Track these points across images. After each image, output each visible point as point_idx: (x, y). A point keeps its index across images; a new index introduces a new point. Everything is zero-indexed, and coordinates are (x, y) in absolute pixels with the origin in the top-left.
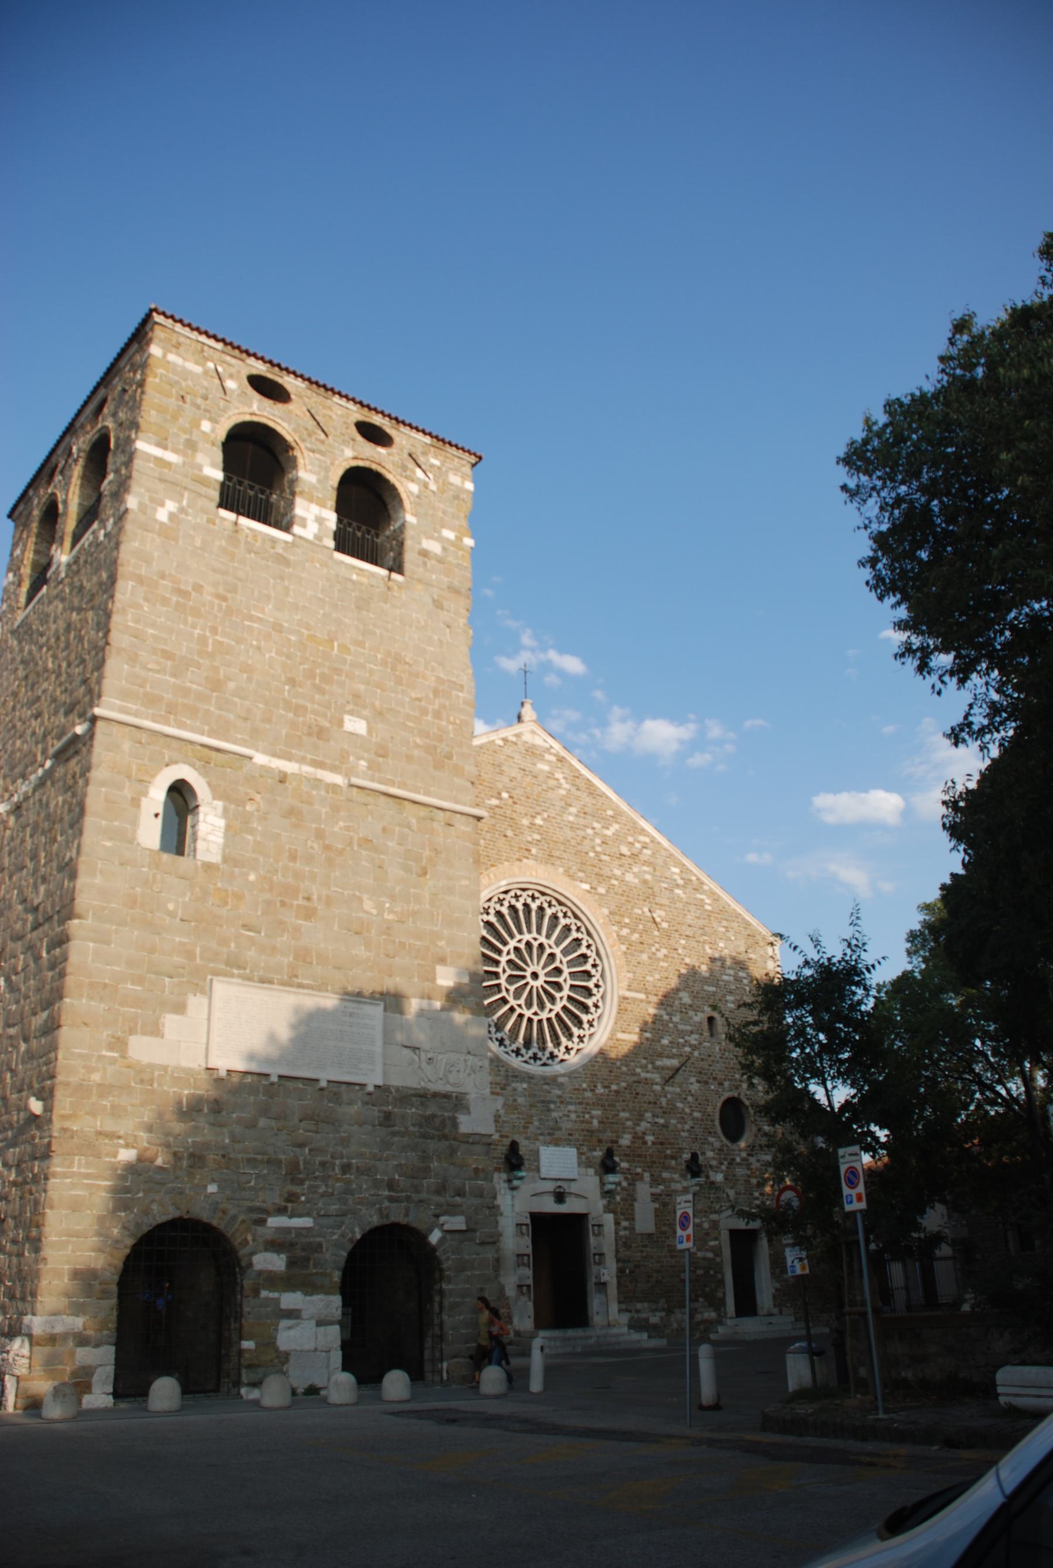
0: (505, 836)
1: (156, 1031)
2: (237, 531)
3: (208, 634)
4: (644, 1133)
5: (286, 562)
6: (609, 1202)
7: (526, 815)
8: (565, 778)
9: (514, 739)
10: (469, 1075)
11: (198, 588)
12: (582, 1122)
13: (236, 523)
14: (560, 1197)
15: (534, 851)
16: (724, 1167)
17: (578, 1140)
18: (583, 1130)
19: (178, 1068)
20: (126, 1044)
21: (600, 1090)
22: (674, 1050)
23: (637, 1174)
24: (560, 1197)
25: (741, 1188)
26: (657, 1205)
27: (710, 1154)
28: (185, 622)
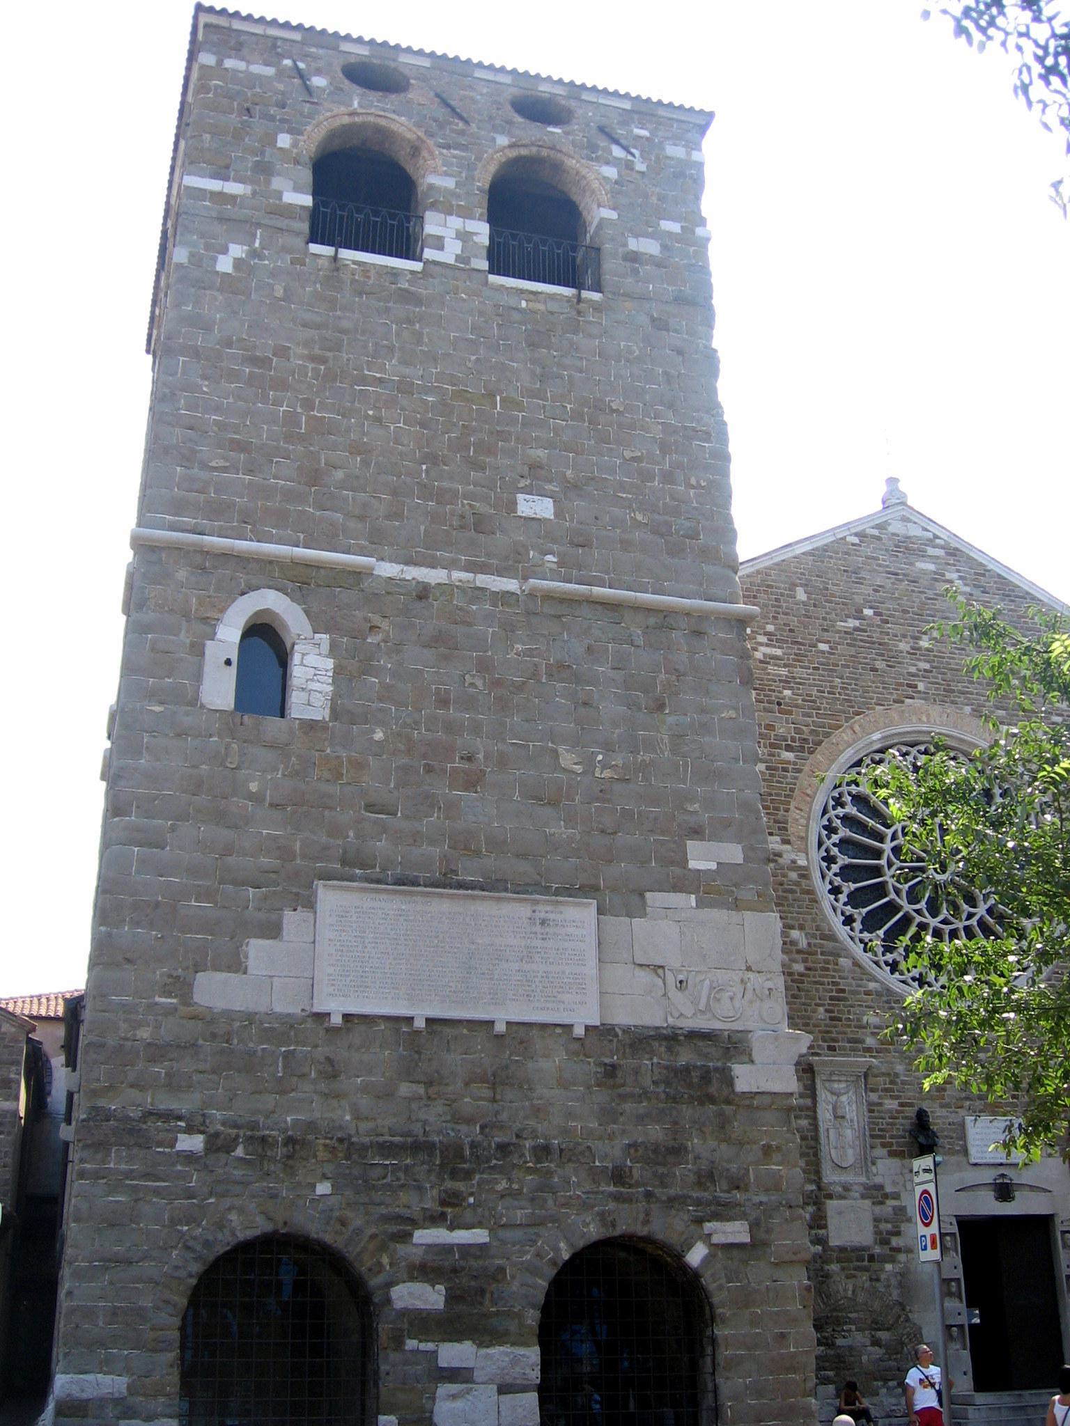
0: (874, 670)
1: (236, 965)
2: (337, 270)
3: (299, 410)
5: (416, 300)
7: (904, 636)
8: (961, 578)
9: (875, 532)
10: (751, 1002)
11: (282, 352)
13: (335, 258)
14: (1004, 1191)
15: (921, 687)
19: (271, 1015)
20: (191, 986)
28: (265, 400)
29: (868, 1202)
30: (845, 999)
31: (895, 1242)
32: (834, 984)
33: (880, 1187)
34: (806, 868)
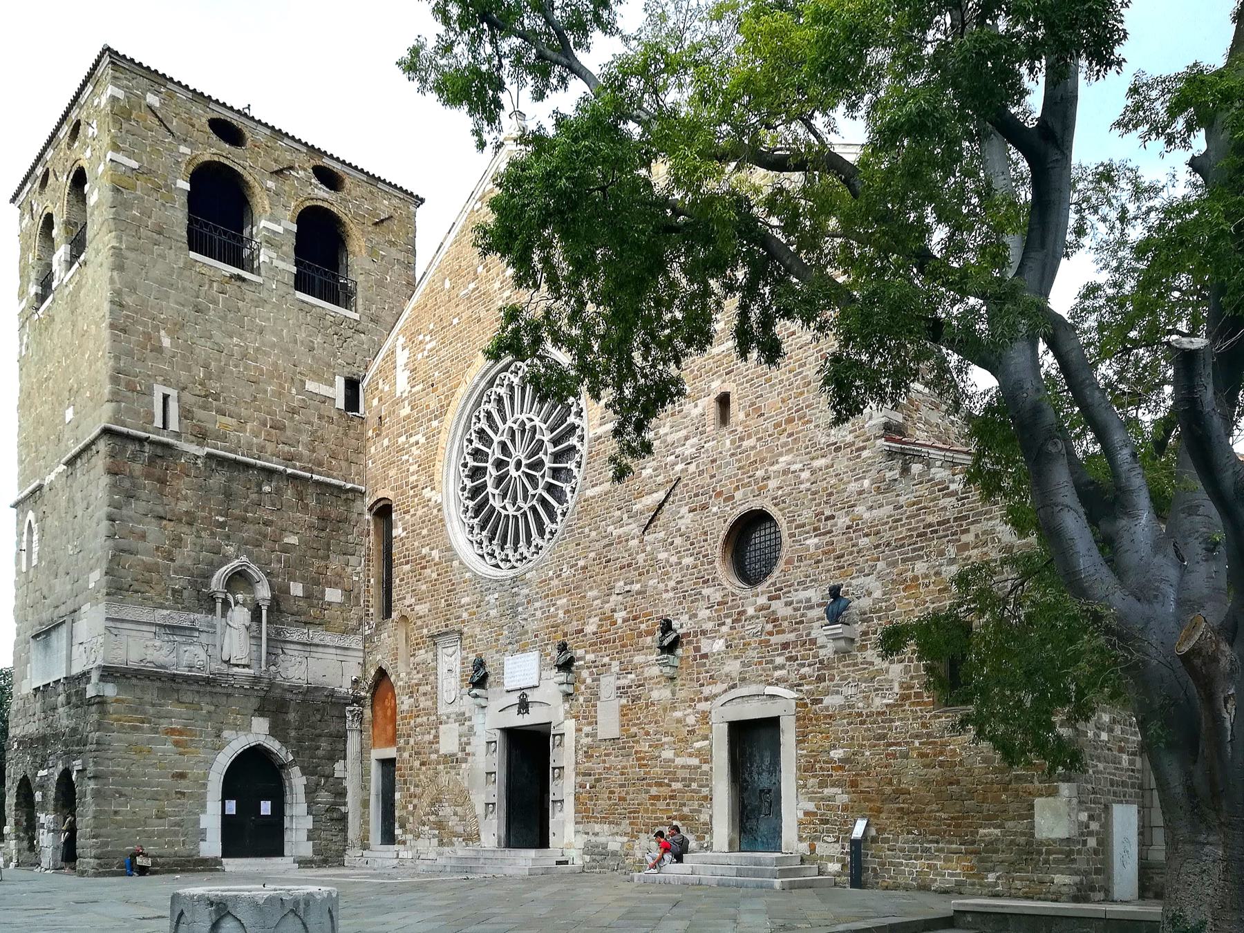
4: (613, 611)
12: (548, 618)
16: (725, 629)
17: (543, 640)
21: (567, 572)
25: (752, 654)
26: (624, 701)
27: (704, 613)
30: (455, 589)
32: (451, 580)
34: (440, 504)
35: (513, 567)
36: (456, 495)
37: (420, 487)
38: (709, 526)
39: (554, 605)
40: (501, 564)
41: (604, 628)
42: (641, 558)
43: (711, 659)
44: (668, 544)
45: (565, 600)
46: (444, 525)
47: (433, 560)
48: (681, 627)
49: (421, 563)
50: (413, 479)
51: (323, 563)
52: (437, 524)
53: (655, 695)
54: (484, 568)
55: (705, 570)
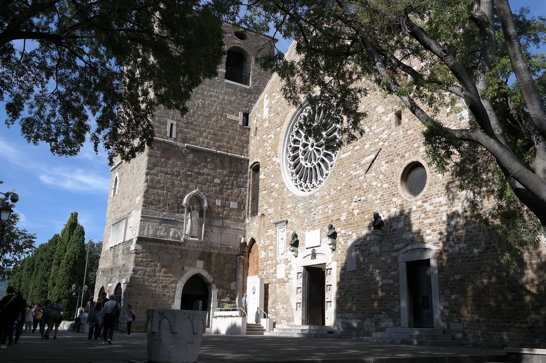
4: (353, 209)
6: (335, 255)
17: (322, 224)
18: (324, 218)
22: (373, 149)
23: (349, 235)
24: (314, 255)
29: (285, 264)
30: (285, 201)
31: (289, 276)
32: (283, 197)
33: (287, 259)
34: (280, 164)
35: (310, 191)
36: (286, 159)
37: (271, 157)
38: (394, 169)
39: (327, 207)
40: (305, 189)
41: (349, 218)
42: (365, 185)
43: (397, 232)
44: (376, 178)
45: (332, 205)
46: (281, 173)
47: (276, 188)
48: (384, 216)
49: (271, 190)
50: (268, 153)
51: (230, 191)
52: (278, 172)
53: (372, 249)
54: (297, 192)
55: (393, 189)
